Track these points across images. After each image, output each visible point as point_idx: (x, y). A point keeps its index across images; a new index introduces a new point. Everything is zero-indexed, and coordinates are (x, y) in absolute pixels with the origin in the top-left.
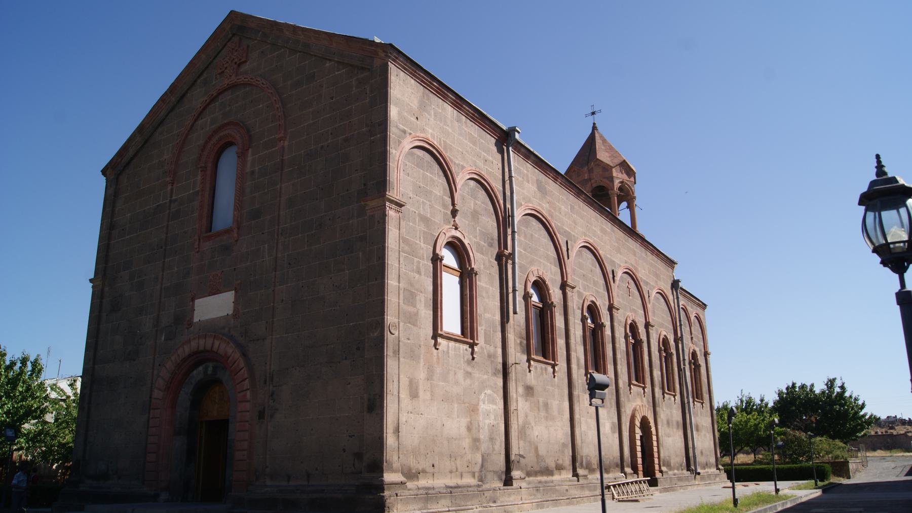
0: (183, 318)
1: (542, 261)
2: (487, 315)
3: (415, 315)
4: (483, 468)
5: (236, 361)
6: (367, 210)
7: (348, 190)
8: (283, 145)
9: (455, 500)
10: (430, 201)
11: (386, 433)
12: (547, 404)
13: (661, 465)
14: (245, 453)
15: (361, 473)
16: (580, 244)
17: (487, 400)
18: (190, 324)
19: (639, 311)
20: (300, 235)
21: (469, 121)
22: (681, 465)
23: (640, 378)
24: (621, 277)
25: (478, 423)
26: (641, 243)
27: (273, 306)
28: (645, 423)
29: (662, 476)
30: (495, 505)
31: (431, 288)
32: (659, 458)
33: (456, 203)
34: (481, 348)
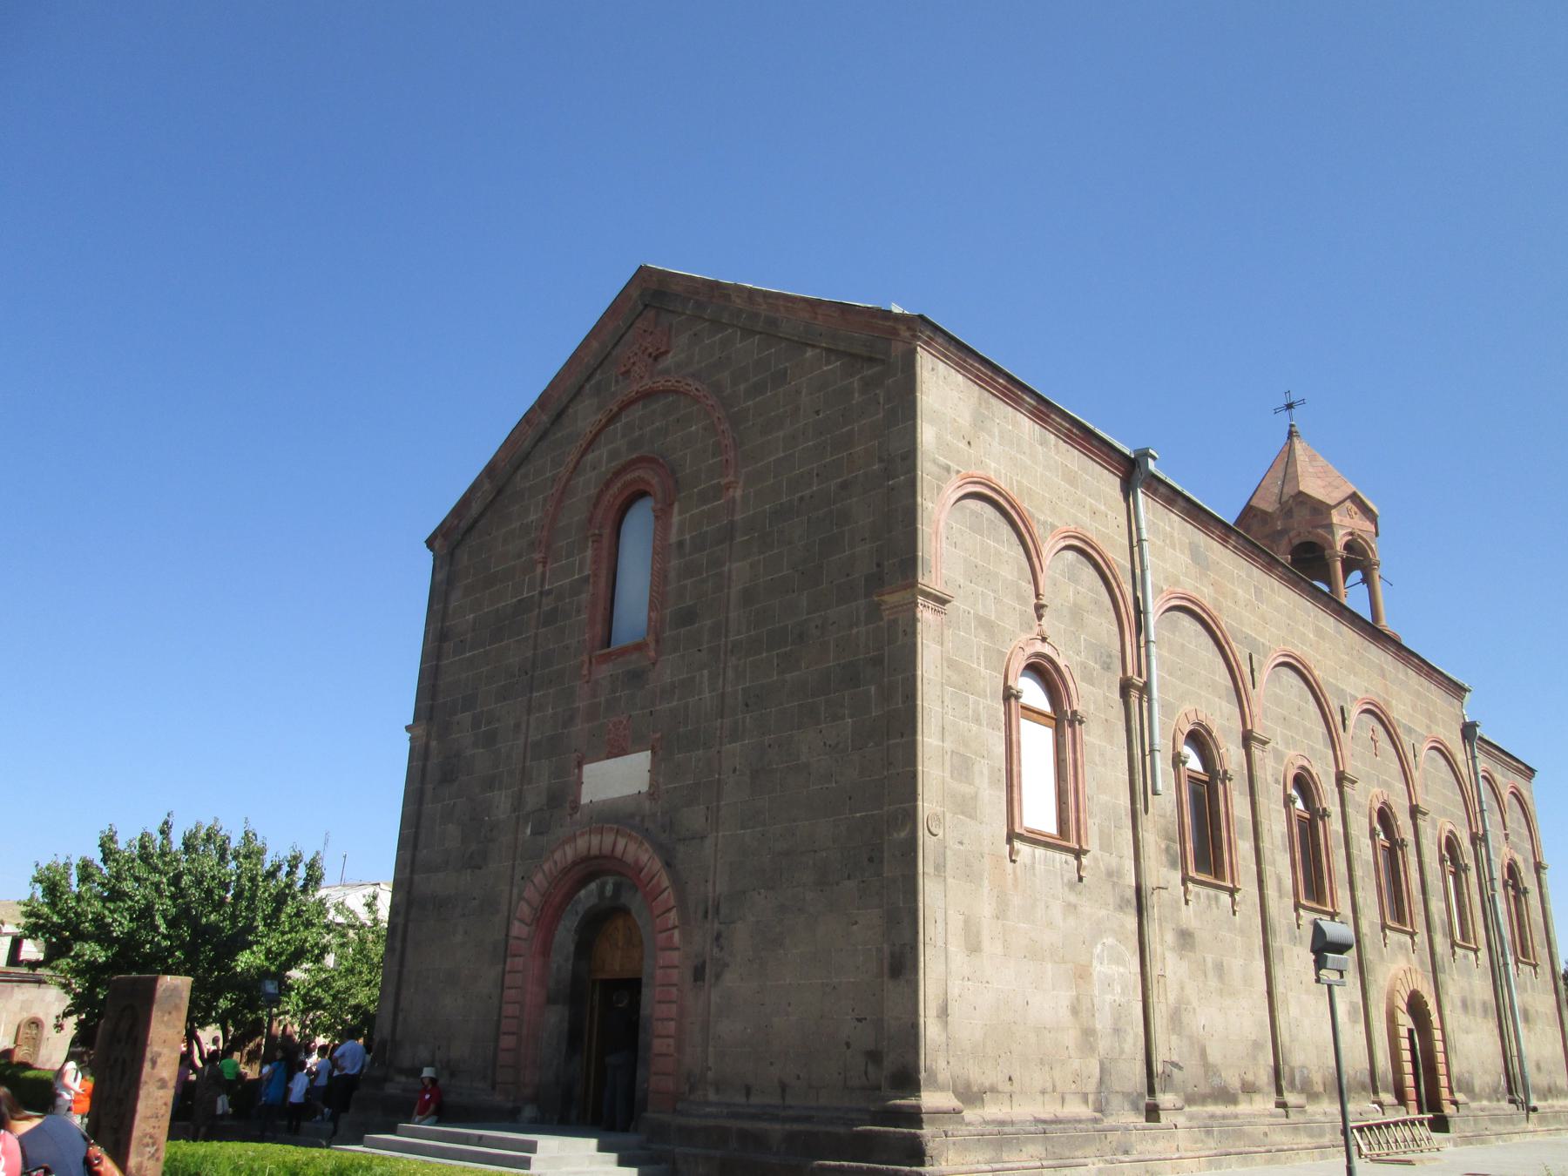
0: (563, 797)
1: (1203, 693)
2: (1104, 798)
3: (972, 798)
4: (1104, 1086)
5: (656, 874)
6: (884, 610)
7: (848, 575)
8: (734, 497)
9: (1053, 1146)
10: (994, 591)
11: (925, 1017)
12: (1222, 966)
13: (1455, 1089)
14: (671, 1041)
15: (879, 1088)
16: (1275, 659)
17: (1107, 957)
18: (576, 807)
19: (1397, 784)
20: (764, 655)
21: (1061, 442)
22: (1496, 1091)
23: (1399, 916)
24: (1358, 720)
25: (1092, 999)
26: (1396, 654)
27: (719, 780)
28: (1416, 1005)
29: (1458, 1111)
30: (1127, 1160)
31: (1002, 749)
32: (1448, 1075)
33: (1041, 592)
34: (1096, 859)
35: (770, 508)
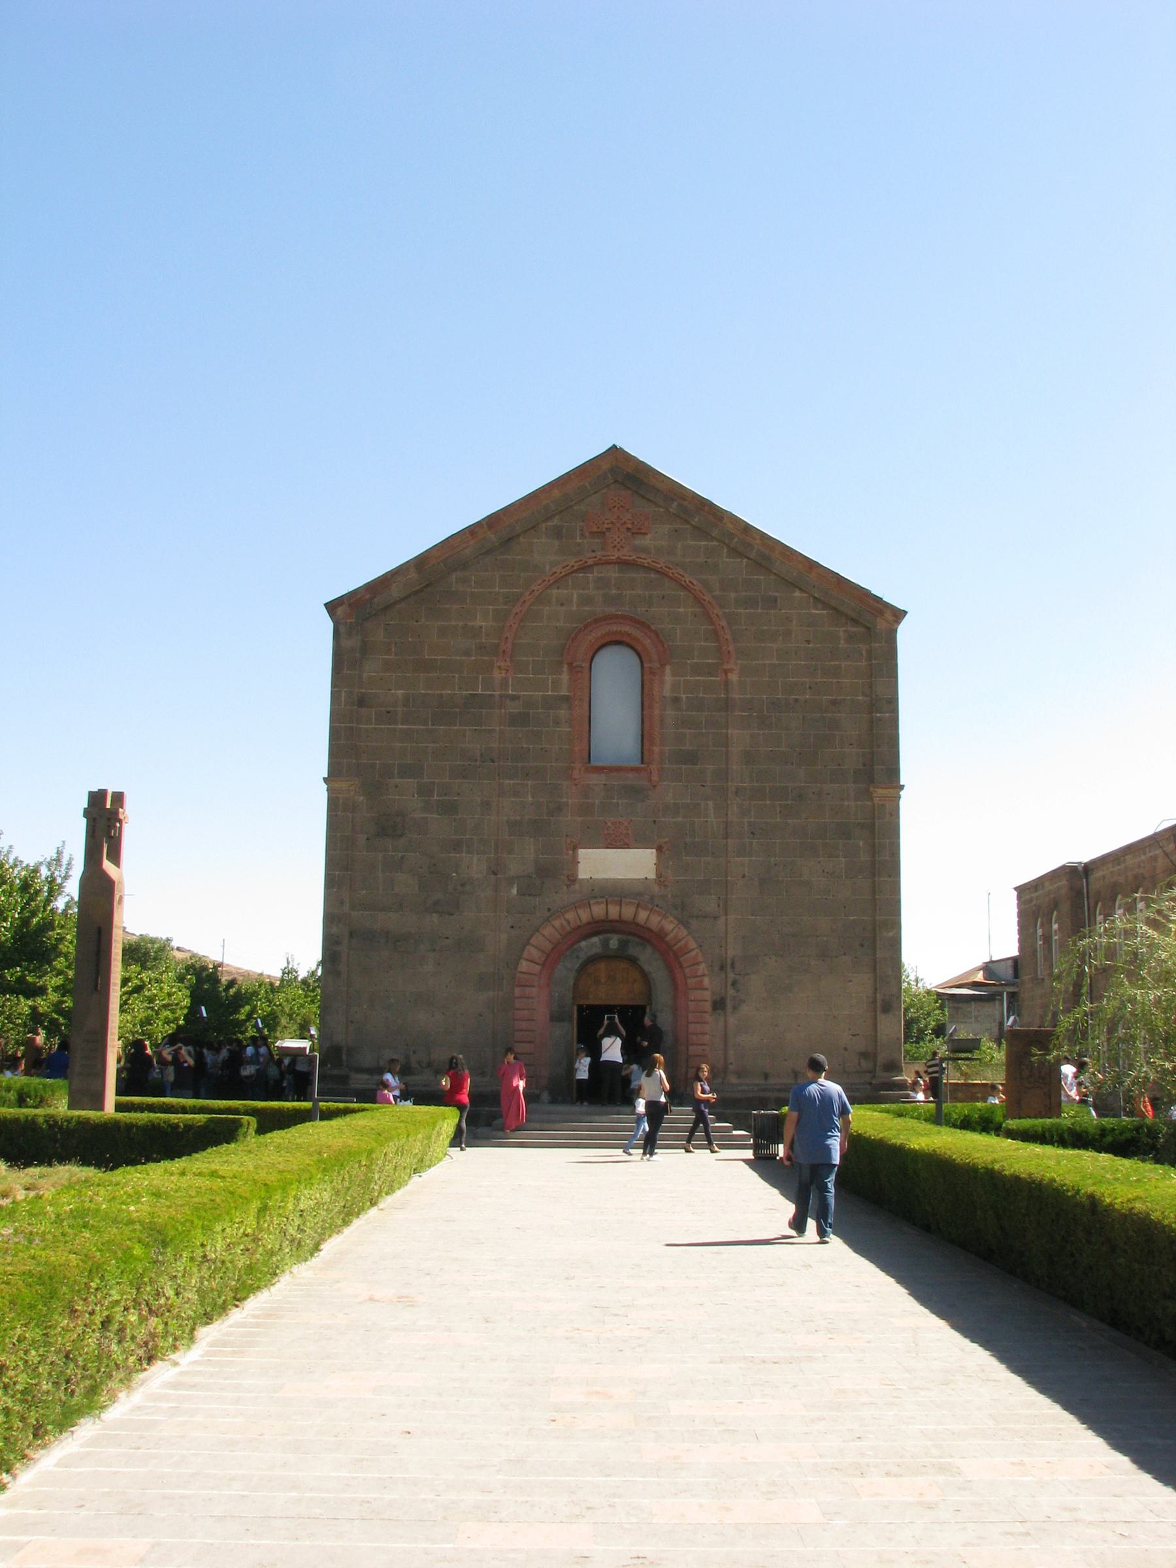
35: (767, 698)
